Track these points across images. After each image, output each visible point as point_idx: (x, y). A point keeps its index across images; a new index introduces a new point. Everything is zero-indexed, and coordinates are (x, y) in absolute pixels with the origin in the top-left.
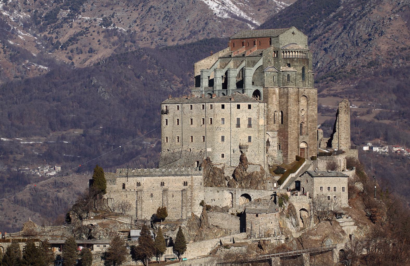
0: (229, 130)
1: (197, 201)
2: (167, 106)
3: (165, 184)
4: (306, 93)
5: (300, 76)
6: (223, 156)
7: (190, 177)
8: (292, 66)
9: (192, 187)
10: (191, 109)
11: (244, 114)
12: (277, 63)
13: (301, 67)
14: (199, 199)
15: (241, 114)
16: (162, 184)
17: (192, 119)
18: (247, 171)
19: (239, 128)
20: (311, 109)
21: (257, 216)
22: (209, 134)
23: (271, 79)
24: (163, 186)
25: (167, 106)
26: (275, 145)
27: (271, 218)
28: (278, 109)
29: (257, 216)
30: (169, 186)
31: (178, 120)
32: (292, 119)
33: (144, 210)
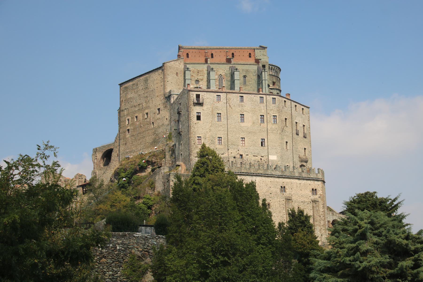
2: (198, 96)
3: (287, 191)
16: (283, 188)
22: (272, 137)
24: (285, 193)
25: (198, 96)
30: (292, 193)
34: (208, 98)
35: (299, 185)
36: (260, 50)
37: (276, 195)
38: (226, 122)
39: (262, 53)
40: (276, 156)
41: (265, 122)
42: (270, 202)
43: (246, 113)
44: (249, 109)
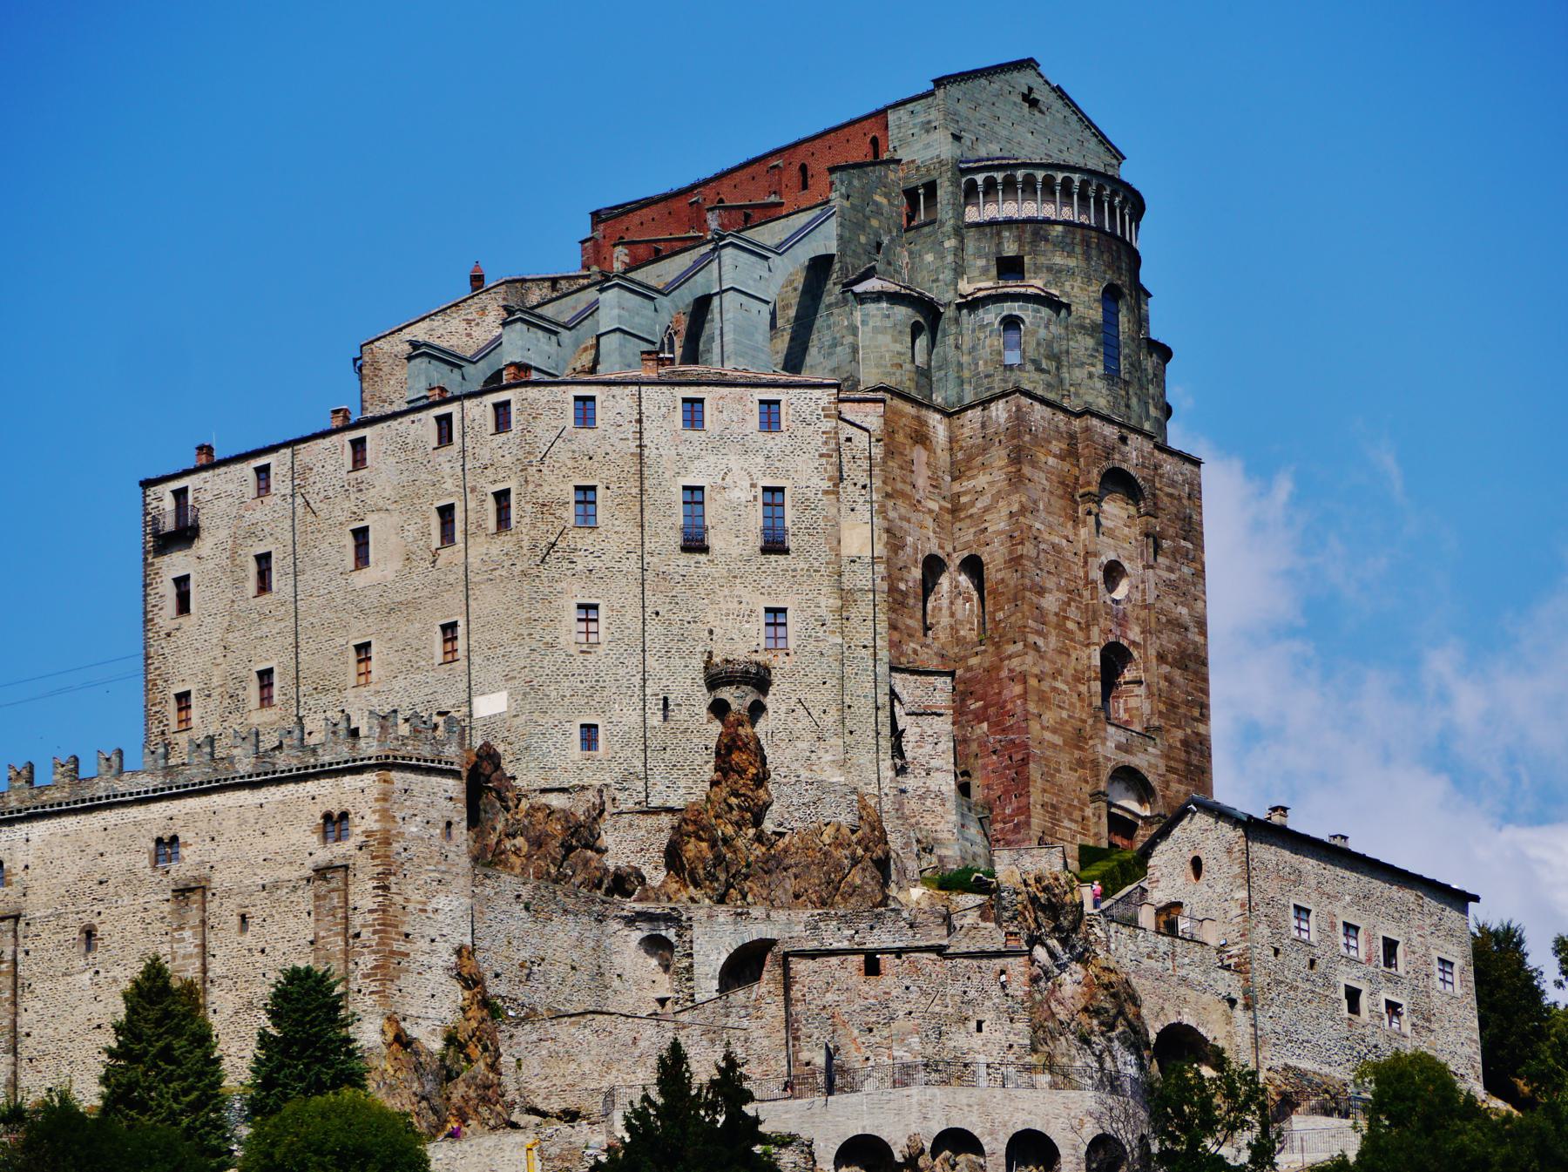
0: (632, 564)
1: (424, 944)
2: (180, 494)
3: (184, 852)
4: (1134, 454)
5: (1090, 342)
6: (589, 734)
7: (369, 778)
8: (1037, 269)
9: (387, 842)
10: (359, 460)
11: (734, 462)
12: (929, 258)
13: (1096, 289)
14: (433, 933)
15: (712, 459)
16: (167, 846)
17: (361, 535)
18: (768, 826)
19: (702, 558)
20: (1166, 575)
21: (872, 967)
22: (487, 601)
23: (898, 347)
24: (174, 866)
25: (180, 494)
26: (934, 763)
27: (972, 994)
28: (949, 549)
29: (872, 967)
31: (264, 560)
32: (1050, 602)
33: (27, 1047)
34: (218, 497)
35: (251, 816)
36: (910, 107)
37: (127, 883)
38: (290, 589)
39: (922, 118)
40: (505, 694)
41: (458, 536)
42: (96, 921)
43: (375, 516)
44: (386, 494)
